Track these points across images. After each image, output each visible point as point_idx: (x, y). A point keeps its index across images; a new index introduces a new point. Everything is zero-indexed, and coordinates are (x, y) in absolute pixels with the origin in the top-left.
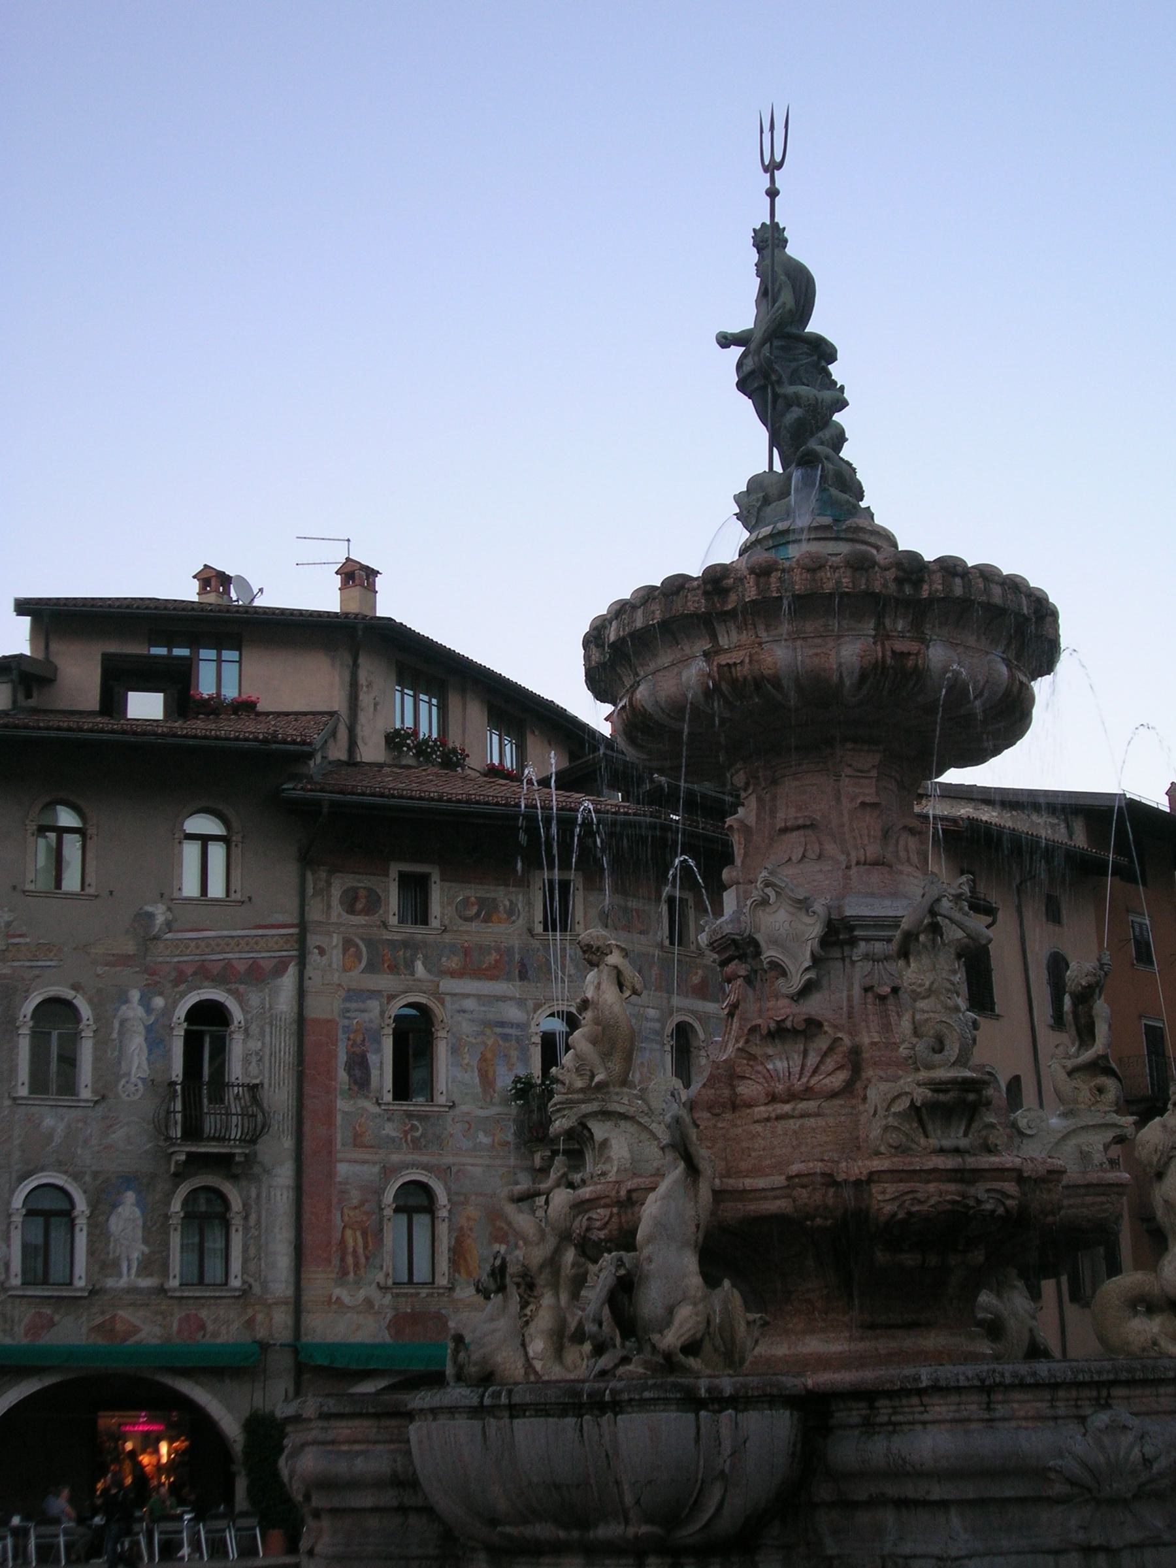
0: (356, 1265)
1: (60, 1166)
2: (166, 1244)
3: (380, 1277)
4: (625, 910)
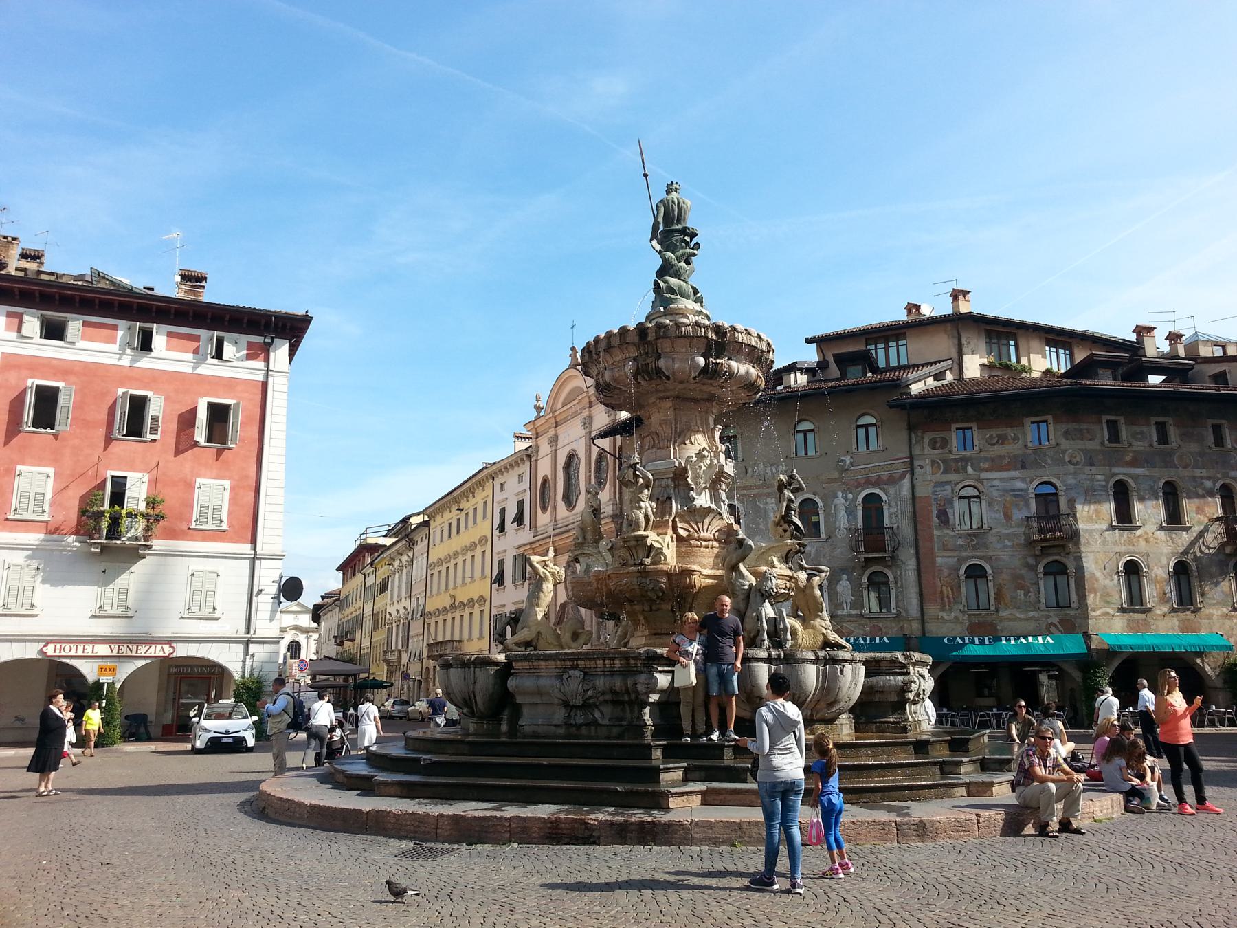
3: (961, 607)
4: (1081, 430)
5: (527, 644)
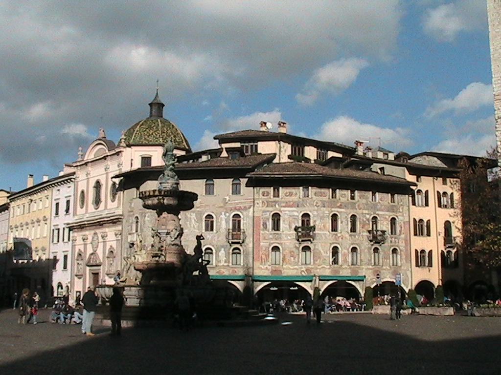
0: (264, 261)
1: (210, 244)
2: (229, 257)
3: (269, 263)
5: (123, 282)
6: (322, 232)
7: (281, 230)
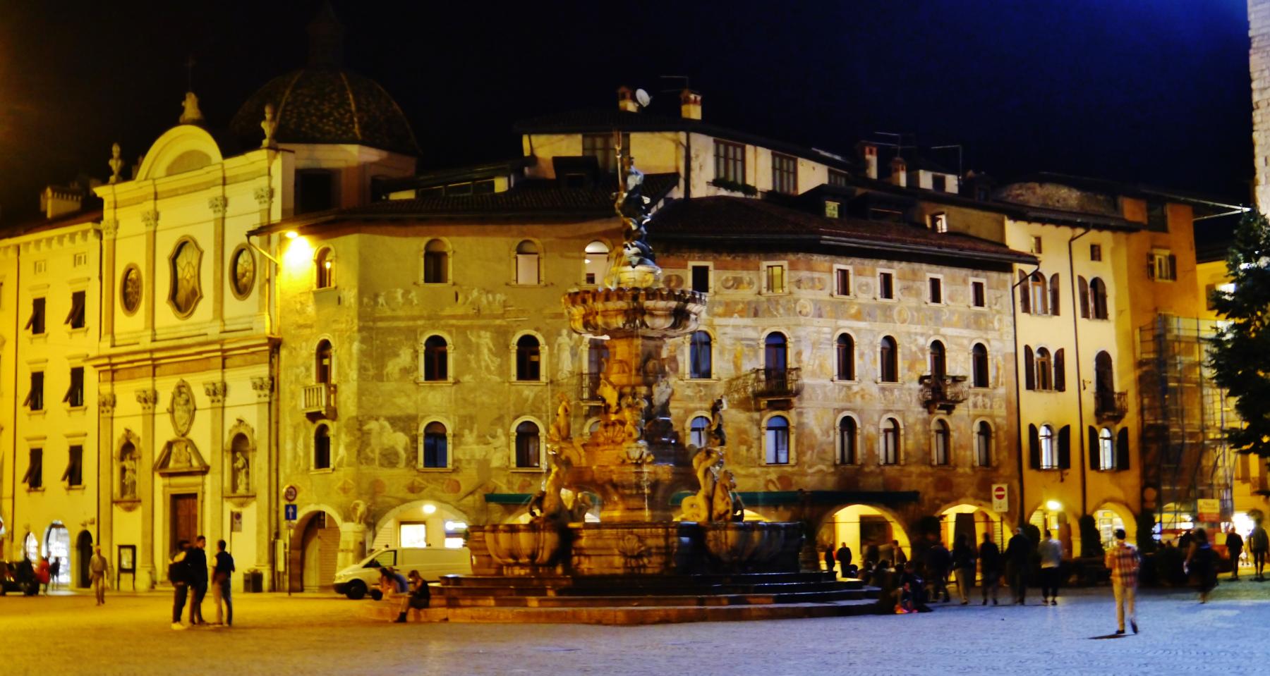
1: (532, 413)
4: (812, 279)
6: (819, 381)
7: (714, 377)
